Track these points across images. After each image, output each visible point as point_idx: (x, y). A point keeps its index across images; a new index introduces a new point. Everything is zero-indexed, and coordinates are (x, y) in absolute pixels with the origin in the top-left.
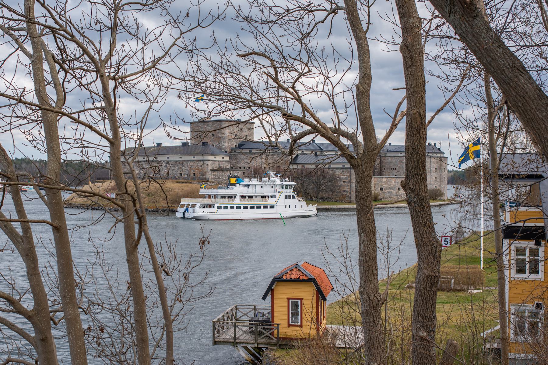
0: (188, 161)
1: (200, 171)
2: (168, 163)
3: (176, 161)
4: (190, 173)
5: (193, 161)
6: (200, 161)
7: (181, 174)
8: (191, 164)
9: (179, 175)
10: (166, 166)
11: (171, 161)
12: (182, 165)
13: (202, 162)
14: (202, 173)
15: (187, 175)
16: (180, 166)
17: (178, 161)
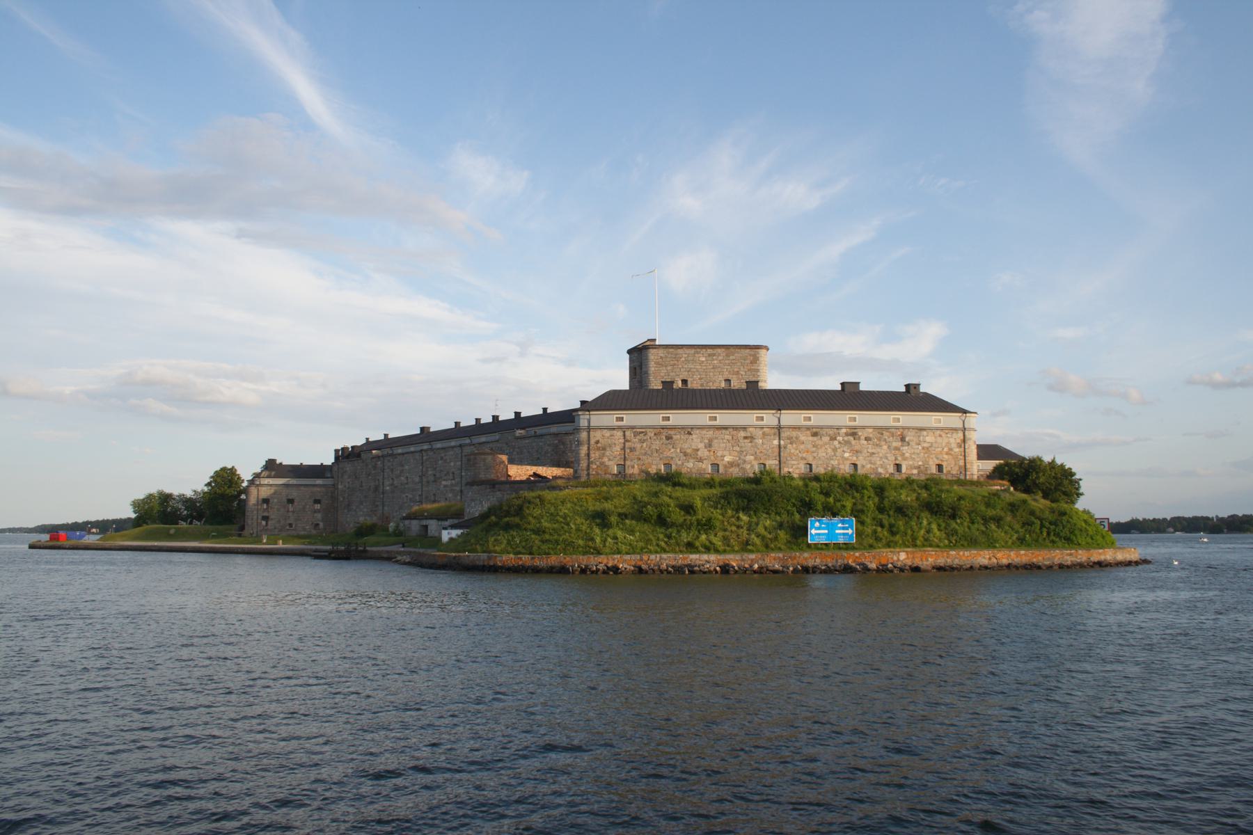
0: (922, 429)
1: (956, 458)
2: (854, 434)
3: (880, 430)
4: (926, 462)
5: (937, 429)
6: (955, 430)
7: (898, 467)
8: (930, 439)
9: (891, 469)
10: (847, 443)
11: (864, 428)
12: (903, 439)
13: (960, 435)
14: (961, 463)
15: (919, 467)
16: (897, 444)
17: (887, 428)
